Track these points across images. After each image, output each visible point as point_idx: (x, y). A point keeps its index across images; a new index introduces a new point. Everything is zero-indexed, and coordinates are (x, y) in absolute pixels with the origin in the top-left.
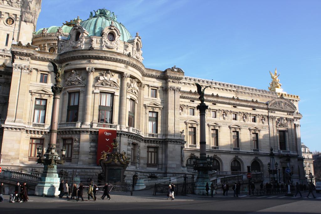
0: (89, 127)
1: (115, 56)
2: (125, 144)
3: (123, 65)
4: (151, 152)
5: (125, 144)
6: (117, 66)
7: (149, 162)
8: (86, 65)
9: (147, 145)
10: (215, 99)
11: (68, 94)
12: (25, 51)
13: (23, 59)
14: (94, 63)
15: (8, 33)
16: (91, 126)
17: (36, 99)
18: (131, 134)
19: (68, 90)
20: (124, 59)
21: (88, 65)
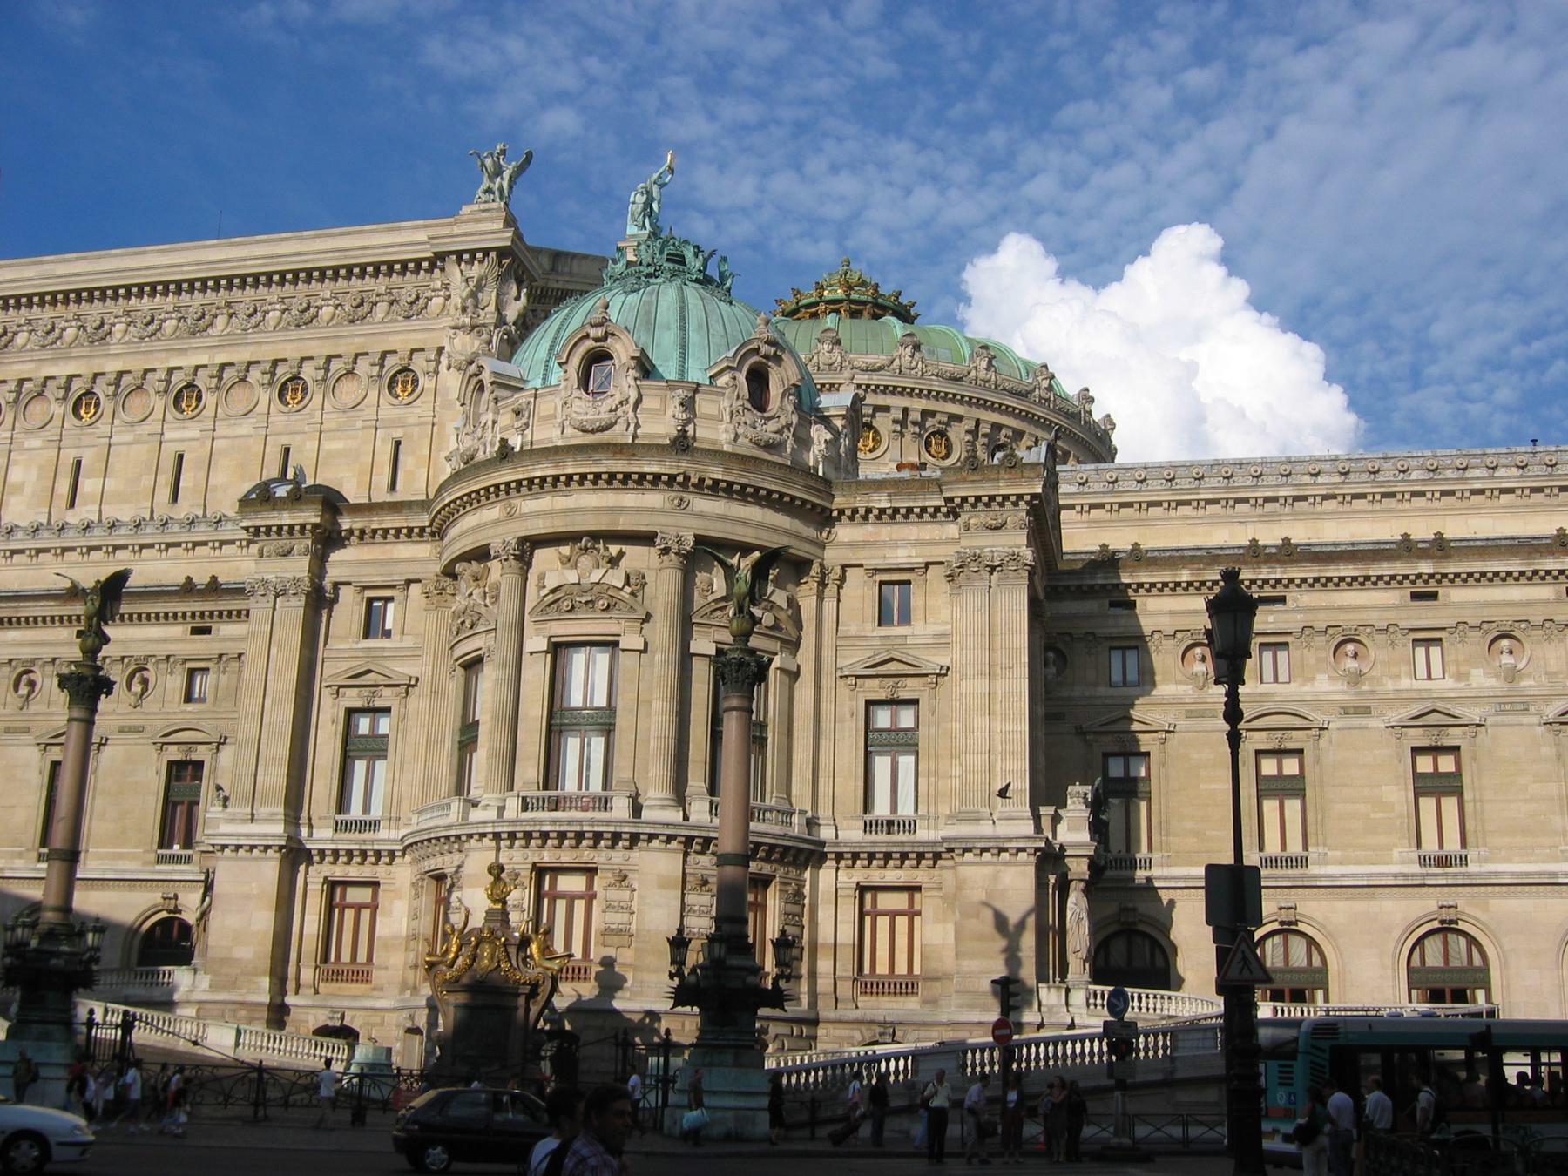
0: (492, 814)
1: (597, 462)
2: (664, 884)
3: (654, 499)
4: (893, 915)
5: (664, 884)
6: (621, 510)
7: (882, 969)
8: (491, 532)
9: (859, 875)
10: (1425, 568)
11: (460, 672)
12: (286, 518)
13: (288, 553)
14: (523, 516)
15: (398, 434)
16: (501, 809)
17: (351, 712)
18: (695, 833)
19: (459, 651)
20: (646, 469)
21: (500, 529)
